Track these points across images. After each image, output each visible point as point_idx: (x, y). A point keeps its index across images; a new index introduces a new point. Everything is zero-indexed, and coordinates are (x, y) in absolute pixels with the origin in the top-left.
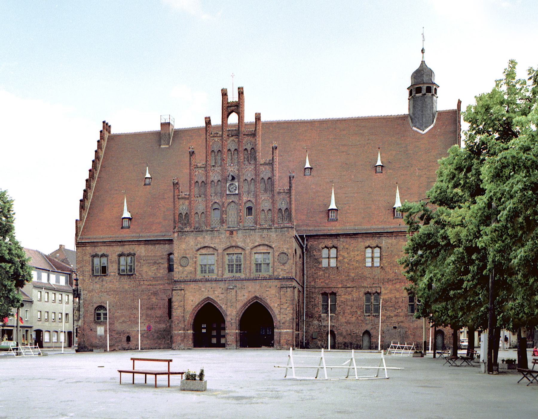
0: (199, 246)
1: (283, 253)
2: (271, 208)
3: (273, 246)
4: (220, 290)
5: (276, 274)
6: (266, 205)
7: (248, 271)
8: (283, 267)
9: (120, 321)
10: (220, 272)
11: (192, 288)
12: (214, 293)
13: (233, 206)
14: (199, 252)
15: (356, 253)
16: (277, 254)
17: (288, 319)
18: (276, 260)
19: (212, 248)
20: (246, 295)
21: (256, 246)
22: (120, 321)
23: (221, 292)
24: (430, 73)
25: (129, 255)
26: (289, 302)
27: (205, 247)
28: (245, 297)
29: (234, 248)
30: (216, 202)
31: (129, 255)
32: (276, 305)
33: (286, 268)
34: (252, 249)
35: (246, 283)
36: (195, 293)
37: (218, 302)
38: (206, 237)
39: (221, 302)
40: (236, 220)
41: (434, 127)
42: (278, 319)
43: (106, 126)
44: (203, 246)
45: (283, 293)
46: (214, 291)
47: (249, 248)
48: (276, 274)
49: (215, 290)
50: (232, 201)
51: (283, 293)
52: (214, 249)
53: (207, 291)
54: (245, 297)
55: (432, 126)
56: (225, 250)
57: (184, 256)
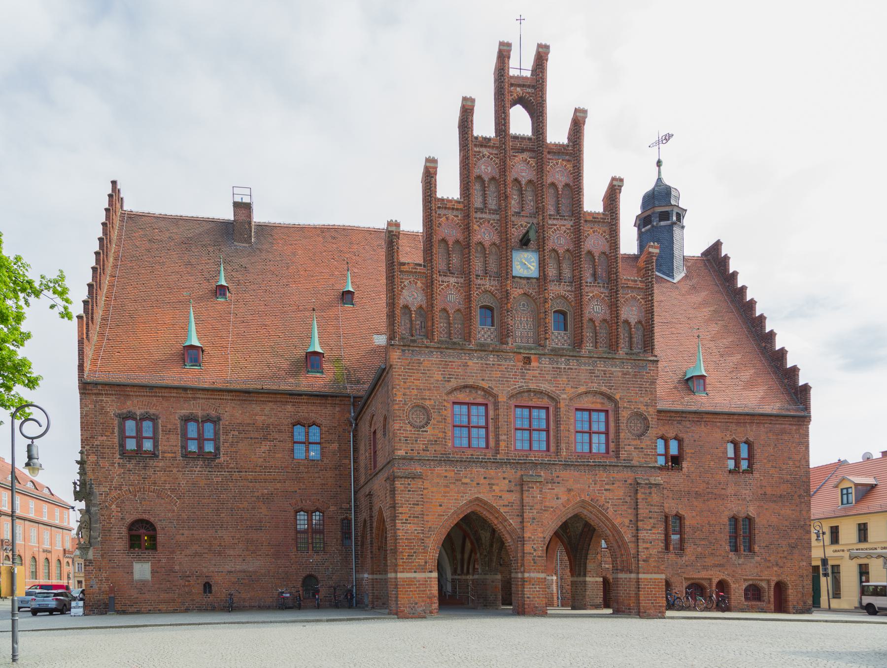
0: (454, 383)
3: (617, 397)
8: (638, 442)
9: (188, 552)
11: (439, 476)
13: (524, 305)
14: (452, 398)
17: (654, 552)
18: (623, 426)
19: (483, 389)
20: (564, 498)
21: (580, 395)
22: (188, 552)
23: (507, 488)
26: (655, 515)
27: (466, 387)
28: (560, 501)
32: (627, 522)
33: (643, 445)
34: (571, 399)
35: (565, 474)
36: (447, 487)
38: (470, 363)
39: (507, 509)
40: (531, 334)
42: (633, 551)
44: (461, 382)
45: (643, 496)
47: (565, 396)
48: (623, 455)
49: (493, 482)
51: (643, 496)
52: (487, 392)
54: (560, 501)
57: (420, 402)
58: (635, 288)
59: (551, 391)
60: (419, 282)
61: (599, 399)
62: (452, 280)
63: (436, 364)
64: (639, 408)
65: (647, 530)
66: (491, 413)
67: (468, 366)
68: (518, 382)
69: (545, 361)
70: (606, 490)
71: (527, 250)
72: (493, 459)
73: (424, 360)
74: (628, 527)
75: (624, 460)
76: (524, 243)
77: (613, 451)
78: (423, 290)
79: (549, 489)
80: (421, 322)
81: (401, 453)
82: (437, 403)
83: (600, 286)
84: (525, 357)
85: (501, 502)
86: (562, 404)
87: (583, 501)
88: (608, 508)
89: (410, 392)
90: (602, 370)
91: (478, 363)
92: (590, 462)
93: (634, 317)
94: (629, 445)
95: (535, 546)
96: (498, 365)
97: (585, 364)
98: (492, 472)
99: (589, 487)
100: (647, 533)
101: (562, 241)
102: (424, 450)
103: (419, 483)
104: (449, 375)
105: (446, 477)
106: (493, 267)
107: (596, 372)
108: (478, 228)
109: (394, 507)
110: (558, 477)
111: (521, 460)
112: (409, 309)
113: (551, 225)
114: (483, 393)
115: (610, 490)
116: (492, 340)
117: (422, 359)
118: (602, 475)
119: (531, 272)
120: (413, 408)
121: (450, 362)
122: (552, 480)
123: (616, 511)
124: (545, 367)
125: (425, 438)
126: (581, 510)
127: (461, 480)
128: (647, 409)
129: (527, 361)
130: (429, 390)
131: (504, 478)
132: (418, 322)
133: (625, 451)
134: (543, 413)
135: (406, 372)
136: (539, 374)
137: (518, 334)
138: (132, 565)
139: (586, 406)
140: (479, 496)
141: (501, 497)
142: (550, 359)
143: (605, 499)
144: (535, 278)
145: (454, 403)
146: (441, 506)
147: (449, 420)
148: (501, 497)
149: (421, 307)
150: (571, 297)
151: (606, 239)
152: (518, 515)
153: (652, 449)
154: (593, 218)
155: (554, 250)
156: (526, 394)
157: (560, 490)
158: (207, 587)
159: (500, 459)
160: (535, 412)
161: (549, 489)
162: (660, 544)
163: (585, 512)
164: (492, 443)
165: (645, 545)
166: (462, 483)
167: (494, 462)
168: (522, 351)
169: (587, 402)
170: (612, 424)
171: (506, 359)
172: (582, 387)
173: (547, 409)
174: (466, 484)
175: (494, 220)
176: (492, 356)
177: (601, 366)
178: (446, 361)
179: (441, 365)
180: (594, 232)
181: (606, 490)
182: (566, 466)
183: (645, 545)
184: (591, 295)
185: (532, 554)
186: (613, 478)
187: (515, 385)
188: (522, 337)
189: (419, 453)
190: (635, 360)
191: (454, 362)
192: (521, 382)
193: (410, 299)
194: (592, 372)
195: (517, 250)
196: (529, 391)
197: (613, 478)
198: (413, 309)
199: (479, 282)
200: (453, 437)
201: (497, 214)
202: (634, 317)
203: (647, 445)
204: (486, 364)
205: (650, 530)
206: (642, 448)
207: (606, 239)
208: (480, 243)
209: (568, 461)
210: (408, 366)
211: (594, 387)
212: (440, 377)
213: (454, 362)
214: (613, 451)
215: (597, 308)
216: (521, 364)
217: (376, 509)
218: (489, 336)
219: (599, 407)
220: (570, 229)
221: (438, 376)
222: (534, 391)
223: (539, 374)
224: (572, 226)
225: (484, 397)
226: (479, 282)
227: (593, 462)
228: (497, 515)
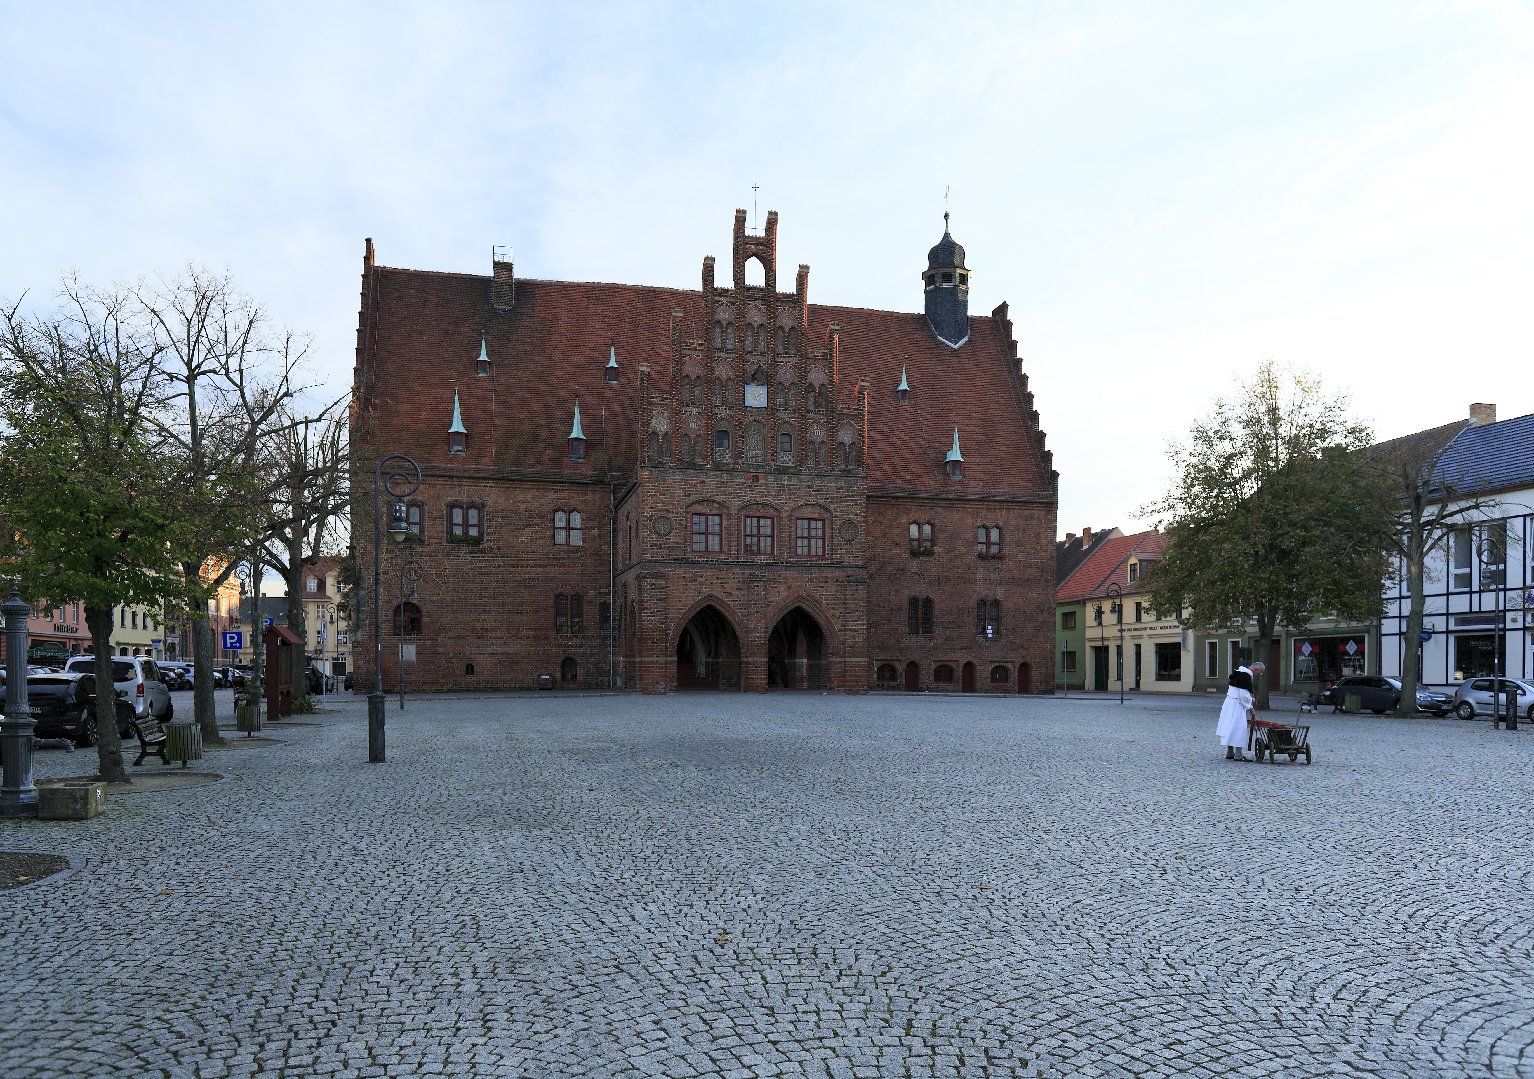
0: (693, 498)
1: (848, 522)
2: (826, 440)
3: (832, 508)
4: (734, 583)
5: (836, 557)
6: (817, 432)
7: (785, 550)
10: (734, 549)
11: (679, 576)
12: (723, 588)
14: (691, 510)
15: (895, 531)
16: (838, 522)
18: (836, 533)
19: (718, 503)
20: (784, 594)
25: (472, 506)
28: (781, 597)
31: (472, 506)
33: (854, 549)
34: (793, 510)
38: (707, 481)
39: (736, 604)
40: (760, 455)
41: (969, 341)
48: (836, 557)
52: (722, 505)
53: (709, 583)
55: (966, 339)
56: (743, 508)
61: (817, 510)
62: (694, 410)
66: (725, 522)
69: (771, 478)
76: (754, 378)
81: (648, 557)
85: (731, 598)
86: (785, 515)
87: (801, 597)
97: (805, 481)
98: (724, 573)
101: (788, 376)
103: (662, 582)
106: (729, 397)
109: (641, 602)
118: (818, 575)
126: (800, 604)
129: (756, 478)
134: (769, 521)
137: (749, 454)
139: (805, 515)
140: (714, 593)
145: (694, 514)
147: (689, 528)
149: (667, 433)
150: (795, 423)
155: (780, 383)
157: (781, 588)
160: (763, 522)
163: (803, 606)
164: (725, 549)
169: (807, 512)
171: (737, 477)
173: (772, 518)
177: (818, 482)
182: (787, 566)
188: (752, 457)
193: (658, 427)
194: (810, 487)
196: (757, 504)
198: (661, 435)
199: (717, 411)
200: (692, 542)
211: (812, 500)
212: (682, 493)
215: (817, 432)
217: (629, 599)
219: (817, 516)
221: (680, 492)
225: (719, 509)
226: (717, 411)
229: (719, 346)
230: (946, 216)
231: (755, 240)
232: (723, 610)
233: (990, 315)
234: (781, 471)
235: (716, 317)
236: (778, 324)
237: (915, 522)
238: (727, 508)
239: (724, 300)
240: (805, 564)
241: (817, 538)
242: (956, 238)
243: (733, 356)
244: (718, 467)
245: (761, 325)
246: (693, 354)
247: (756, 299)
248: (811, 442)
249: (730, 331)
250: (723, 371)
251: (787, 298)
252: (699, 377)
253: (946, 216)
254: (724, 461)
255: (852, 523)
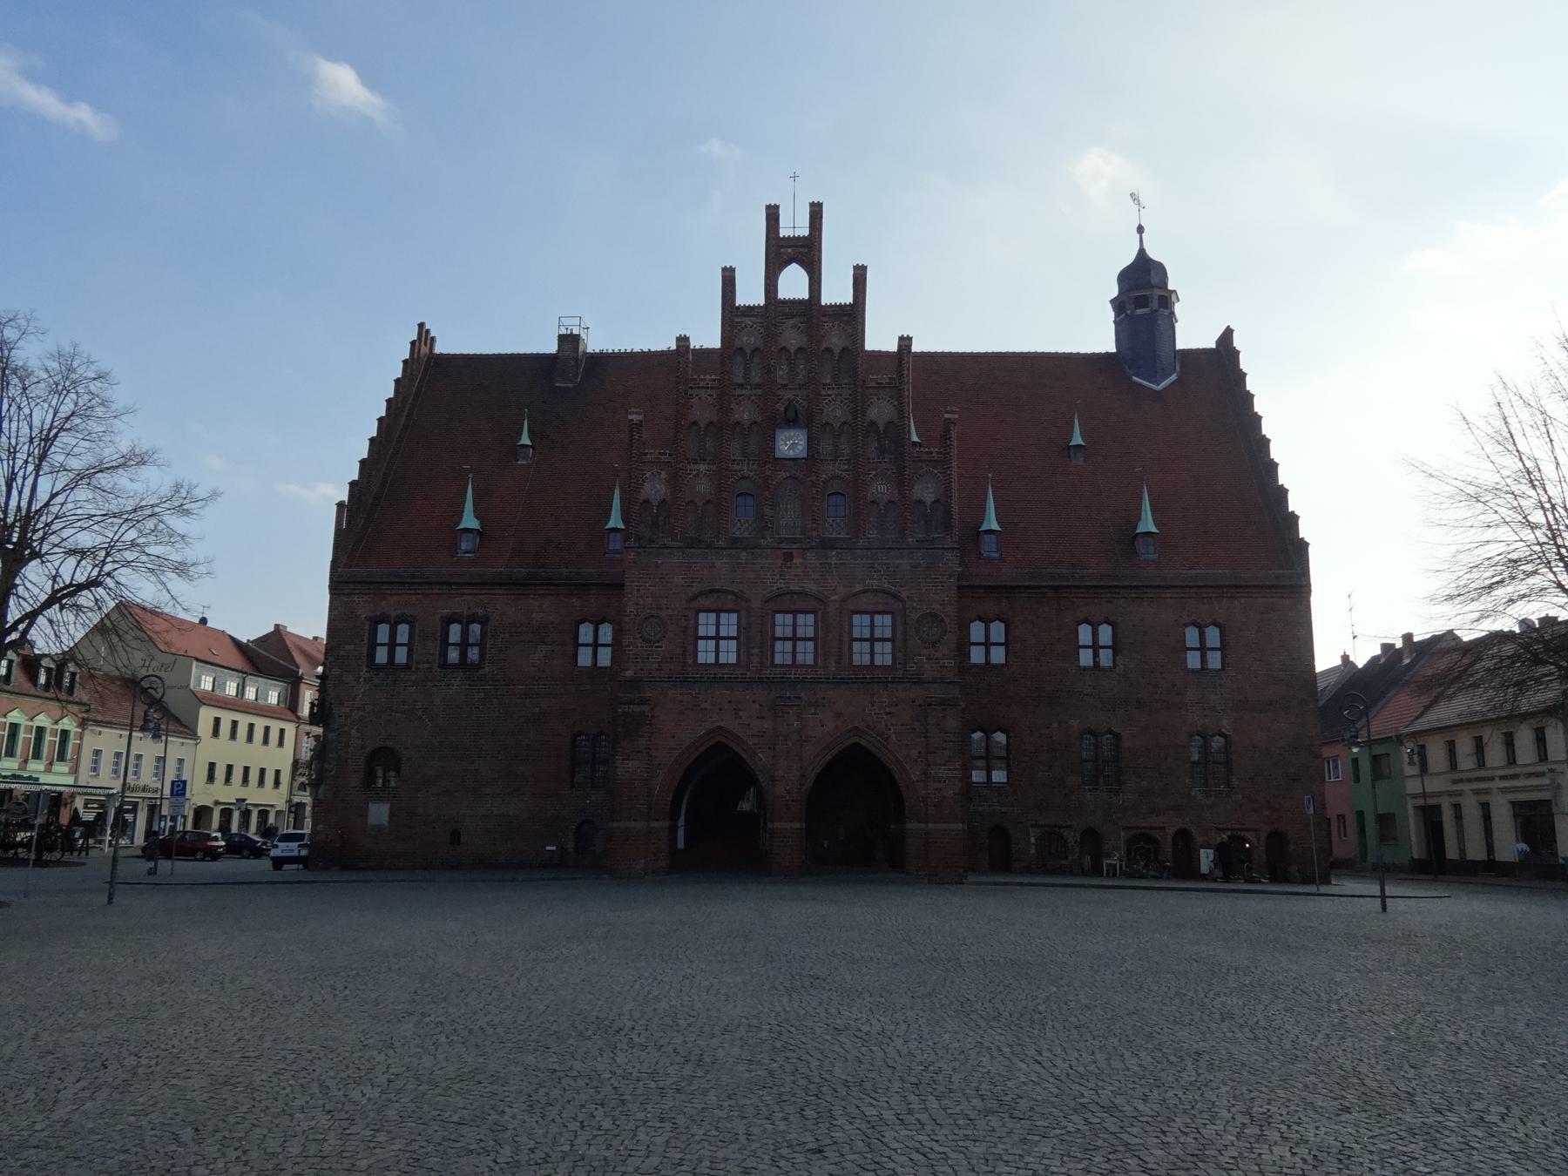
0: (696, 588)
1: (930, 615)
3: (904, 595)
10: (756, 660)
13: (791, 490)
14: (695, 604)
19: (734, 594)
21: (855, 595)
24: (1161, 269)
27: (713, 591)
29: (795, 596)
30: (743, 477)
32: (914, 754)
34: (844, 600)
37: (750, 743)
38: (718, 563)
43: (424, 337)
46: (737, 711)
47: (836, 597)
50: (791, 477)
52: (739, 596)
56: (768, 601)
58: (930, 461)
59: (818, 592)
60: (663, 473)
62: (703, 468)
63: (678, 567)
64: (933, 609)
65: (940, 765)
67: (715, 567)
68: (776, 583)
69: (811, 555)
70: (887, 714)
71: (794, 427)
72: (742, 678)
73: (662, 563)
74: (916, 760)
75: (913, 675)
77: (900, 663)
78: (667, 481)
79: (812, 714)
80: (665, 518)
82: (676, 613)
83: (885, 462)
84: (784, 553)
87: (857, 728)
88: (889, 737)
89: (644, 601)
90: (885, 564)
91: (727, 563)
92: (866, 678)
93: (930, 495)
94: (920, 655)
95: (788, 788)
96: (753, 564)
99: (864, 710)
100: (940, 769)
101: (839, 413)
102: (657, 670)
103: (646, 708)
104: (692, 578)
105: (681, 701)
107: (876, 565)
108: (736, 406)
110: (824, 698)
111: (776, 678)
112: (651, 503)
113: (825, 396)
114: (734, 597)
115: (890, 713)
116: (750, 534)
117: (660, 562)
119: (797, 452)
120: (649, 617)
121: (694, 563)
122: (816, 702)
123: (900, 741)
124: (810, 563)
125: (659, 655)
127: (699, 705)
128: (944, 608)
129: (789, 557)
130: (666, 597)
131: (754, 702)
132: (661, 518)
133: (915, 663)
135: (640, 578)
136: (803, 572)
137: (783, 523)
138: (368, 807)
141: (749, 725)
142: (816, 553)
143: (886, 725)
144: (803, 459)
146: (673, 737)
148: (749, 725)
149: (664, 500)
151: (894, 406)
152: (770, 748)
153: (951, 659)
154: (877, 383)
156: (788, 596)
158: (456, 836)
159: (750, 678)
160: (800, 618)
161: (812, 714)
162: (957, 782)
163: (863, 743)
165: (937, 785)
166: (701, 709)
167: (741, 682)
168: (782, 546)
170: (900, 630)
172: (858, 585)
174: (706, 709)
175: (755, 395)
176: (745, 554)
178: (689, 563)
179: (682, 567)
180: (878, 399)
181: (887, 714)
183: (937, 785)
184: (874, 473)
185: (785, 797)
186: (896, 697)
187: (773, 586)
189: (650, 673)
190: (927, 549)
191: (697, 563)
192: (781, 583)
195: (783, 428)
196: (791, 593)
197: (896, 697)
198: (655, 503)
199: (735, 467)
201: (760, 389)
202: (930, 495)
203: (944, 655)
204: (737, 564)
205: (944, 765)
206: (937, 659)
207: (894, 406)
208: (738, 423)
209: (837, 678)
210: (643, 570)
211: (875, 584)
213: (697, 563)
214: (900, 663)
215: (882, 488)
216: (780, 562)
218: (748, 529)
219: (881, 608)
220: (848, 399)
222: (797, 593)
223: (803, 572)
224: (850, 395)
227: (870, 678)
228: (746, 748)
229: (741, 381)
230: (1140, 229)
231: (794, 241)
232: (740, 751)
233: (1214, 346)
234: (826, 545)
235: (738, 344)
236: (824, 346)
237: (1086, 621)
238: (747, 601)
239: (748, 321)
240: (870, 678)
241: (883, 640)
242: (1153, 254)
243: (759, 392)
244: (734, 544)
245: (800, 349)
246: (703, 394)
247: (792, 316)
248: (873, 502)
249: (756, 360)
250: (745, 413)
251: (838, 311)
252: (711, 423)
253: (1140, 229)
254: (746, 534)
255: (936, 616)
